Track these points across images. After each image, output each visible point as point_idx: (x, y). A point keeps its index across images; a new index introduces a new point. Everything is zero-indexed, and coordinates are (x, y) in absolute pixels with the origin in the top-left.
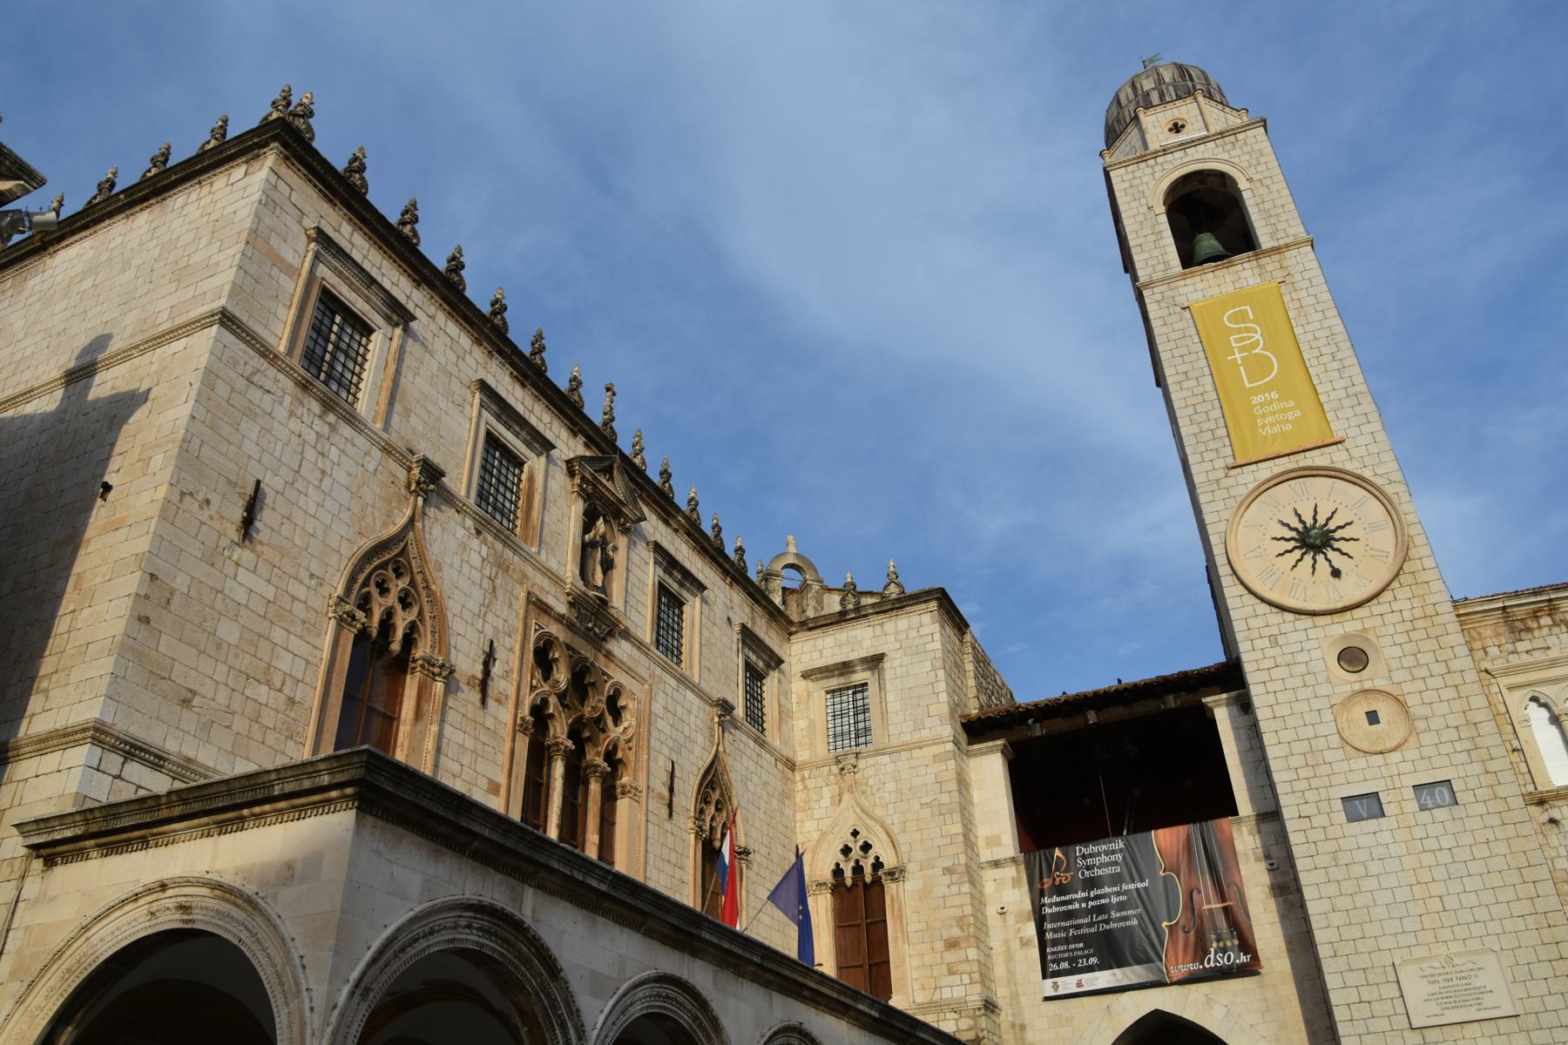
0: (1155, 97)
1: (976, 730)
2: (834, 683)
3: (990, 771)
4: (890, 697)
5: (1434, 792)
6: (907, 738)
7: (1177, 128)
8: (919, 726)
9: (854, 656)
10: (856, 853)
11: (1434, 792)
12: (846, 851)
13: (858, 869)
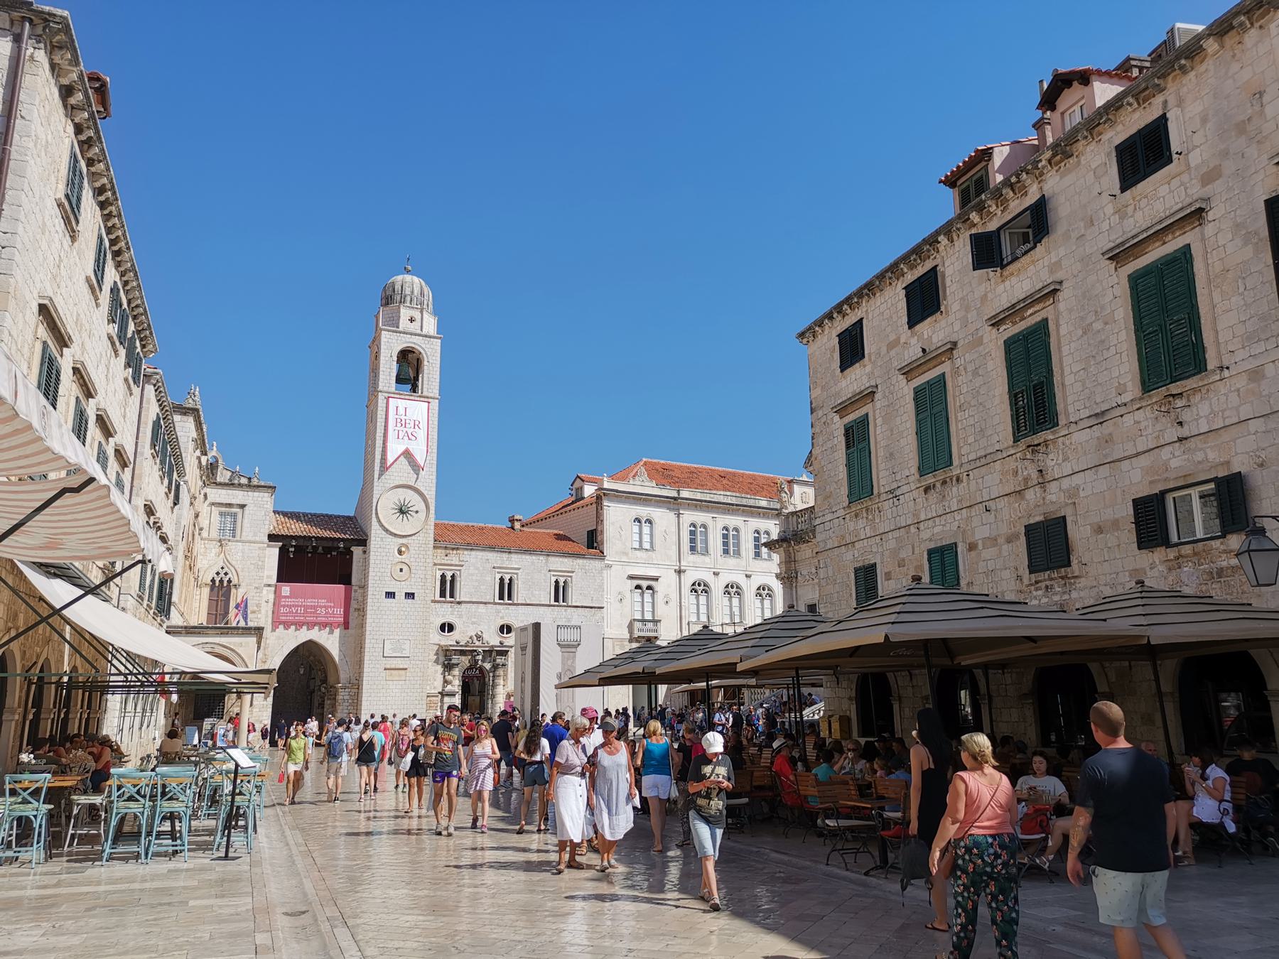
0: (408, 299)
1: (272, 537)
2: (223, 509)
3: (273, 553)
4: (246, 521)
5: (410, 596)
6: (250, 538)
7: (412, 320)
8: (255, 535)
9: (234, 502)
10: (222, 575)
11: (410, 596)
12: (218, 573)
13: (221, 581)
